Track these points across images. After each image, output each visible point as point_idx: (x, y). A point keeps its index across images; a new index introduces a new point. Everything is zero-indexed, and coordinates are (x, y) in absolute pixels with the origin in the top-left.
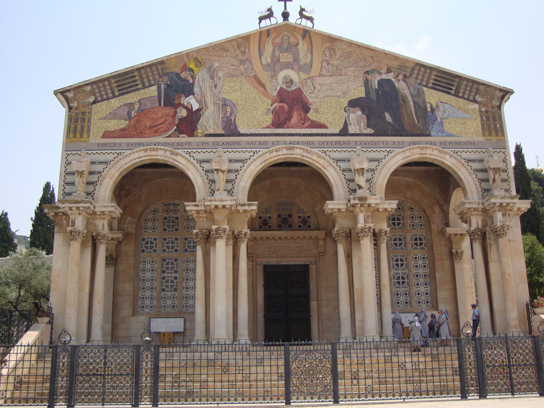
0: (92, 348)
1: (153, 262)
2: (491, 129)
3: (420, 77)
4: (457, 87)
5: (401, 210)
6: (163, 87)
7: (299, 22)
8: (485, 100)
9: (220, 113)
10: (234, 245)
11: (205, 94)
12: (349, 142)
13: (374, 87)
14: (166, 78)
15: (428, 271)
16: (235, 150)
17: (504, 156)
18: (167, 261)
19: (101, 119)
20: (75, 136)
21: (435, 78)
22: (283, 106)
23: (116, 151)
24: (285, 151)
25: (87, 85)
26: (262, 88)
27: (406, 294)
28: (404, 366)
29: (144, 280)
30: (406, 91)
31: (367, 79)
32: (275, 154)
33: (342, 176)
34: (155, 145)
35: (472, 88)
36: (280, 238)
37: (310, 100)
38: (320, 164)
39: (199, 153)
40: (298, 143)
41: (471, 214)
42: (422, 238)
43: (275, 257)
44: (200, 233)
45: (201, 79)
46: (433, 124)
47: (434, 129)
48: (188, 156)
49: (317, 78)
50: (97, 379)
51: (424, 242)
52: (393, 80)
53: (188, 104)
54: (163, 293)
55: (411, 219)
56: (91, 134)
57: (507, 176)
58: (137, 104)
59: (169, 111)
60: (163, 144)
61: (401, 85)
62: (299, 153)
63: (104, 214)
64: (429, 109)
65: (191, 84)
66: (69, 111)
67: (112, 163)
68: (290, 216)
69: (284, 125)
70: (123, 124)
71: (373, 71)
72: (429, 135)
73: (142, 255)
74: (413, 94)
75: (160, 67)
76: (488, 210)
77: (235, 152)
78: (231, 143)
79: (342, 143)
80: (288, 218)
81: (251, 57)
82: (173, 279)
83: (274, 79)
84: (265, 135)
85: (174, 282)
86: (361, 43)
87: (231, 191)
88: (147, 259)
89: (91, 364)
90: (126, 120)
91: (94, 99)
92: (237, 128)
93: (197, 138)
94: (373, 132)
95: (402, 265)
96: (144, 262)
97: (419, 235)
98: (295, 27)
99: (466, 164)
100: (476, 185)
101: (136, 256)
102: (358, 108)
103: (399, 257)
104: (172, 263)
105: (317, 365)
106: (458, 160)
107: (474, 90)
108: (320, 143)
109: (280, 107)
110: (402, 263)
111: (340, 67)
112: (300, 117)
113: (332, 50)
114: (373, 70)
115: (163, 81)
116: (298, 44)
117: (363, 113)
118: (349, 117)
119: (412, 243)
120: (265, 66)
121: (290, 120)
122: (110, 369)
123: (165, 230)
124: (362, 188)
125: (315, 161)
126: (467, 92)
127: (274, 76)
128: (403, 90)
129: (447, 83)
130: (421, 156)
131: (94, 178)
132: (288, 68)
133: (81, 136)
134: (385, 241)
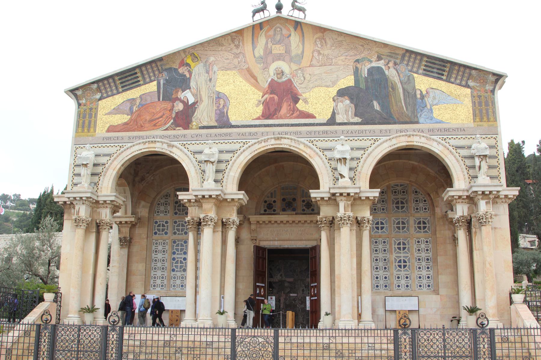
0: (68, 328)
1: (164, 244)
2: (483, 115)
3: (411, 64)
4: (449, 71)
5: (405, 193)
6: (162, 82)
7: (290, 14)
8: (478, 85)
9: (213, 106)
10: (222, 232)
11: (201, 88)
12: (336, 132)
13: (363, 76)
14: (165, 74)
15: (430, 254)
16: (226, 141)
17: (495, 141)
18: (177, 243)
19: (106, 114)
20: (83, 131)
21: (426, 64)
22: (274, 97)
23: (118, 144)
24: (273, 142)
25: (93, 83)
26: (255, 81)
27: (407, 278)
28: (341, 353)
29: (156, 260)
30: (396, 78)
31: (356, 67)
32: (263, 144)
33: (328, 165)
34: (154, 137)
35: (464, 73)
36: (282, 222)
37: (300, 91)
38: (307, 154)
39: (193, 144)
40: (286, 133)
41: (456, 202)
42: (426, 221)
43: (278, 240)
44: (192, 220)
45: (197, 73)
46: (421, 111)
47: (423, 116)
48: (183, 148)
49: (307, 68)
50: (72, 354)
51: (427, 225)
52: (383, 67)
53: (185, 98)
54: (173, 273)
55: (415, 202)
56: (97, 129)
57: (498, 162)
58: (139, 99)
59: (168, 105)
60: (161, 137)
61: (391, 73)
62: (287, 143)
63: (106, 203)
64: (418, 96)
65: (188, 78)
66: (79, 108)
67: (115, 155)
68: (294, 200)
69: (274, 115)
70: (125, 118)
71: (363, 59)
72: (417, 122)
73: (155, 237)
74: (404, 81)
75: (159, 64)
76: (472, 198)
77: (226, 143)
78: (223, 135)
79: (329, 133)
80: (292, 202)
81: (244, 50)
82: (182, 260)
83: (266, 71)
84: (255, 126)
85: (183, 263)
86: (351, 32)
87: (222, 181)
88: (159, 241)
89: (67, 341)
90: (128, 115)
91: (100, 96)
92: (229, 120)
93: (192, 130)
94: (360, 120)
95: (404, 248)
96: (156, 244)
97: (423, 219)
98: (287, 19)
99: (454, 151)
100: (463, 172)
101: (148, 238)
102: (346, 97)
103: (401, 241)
104: (182, 245)
105: (249, 349)
106: (445, 147)
107: (466, 75)
108: (308, 133)
109: (270, 98)
110: (405, 246)
111: (330, 57)
112: (289, 108)
113: (322, 39)
114: (363, 58)
115: (162, 77)
116: (290, 35)
117: (351, 102)
118: (337, 106)
119: (415, 226)
120: (257, 59)
121: (280, 111)
122: (82, 346)
123: (176, 213)
124: (344, 177)
125: (302, 150)
126: (459, 77)
127: (266, 68)
128: (393, 77)
129: (438, 69)
130: (408, 144)
131: (99, 169)
132: (279, 59)
133: (89, 131)
134: (368, 228)
